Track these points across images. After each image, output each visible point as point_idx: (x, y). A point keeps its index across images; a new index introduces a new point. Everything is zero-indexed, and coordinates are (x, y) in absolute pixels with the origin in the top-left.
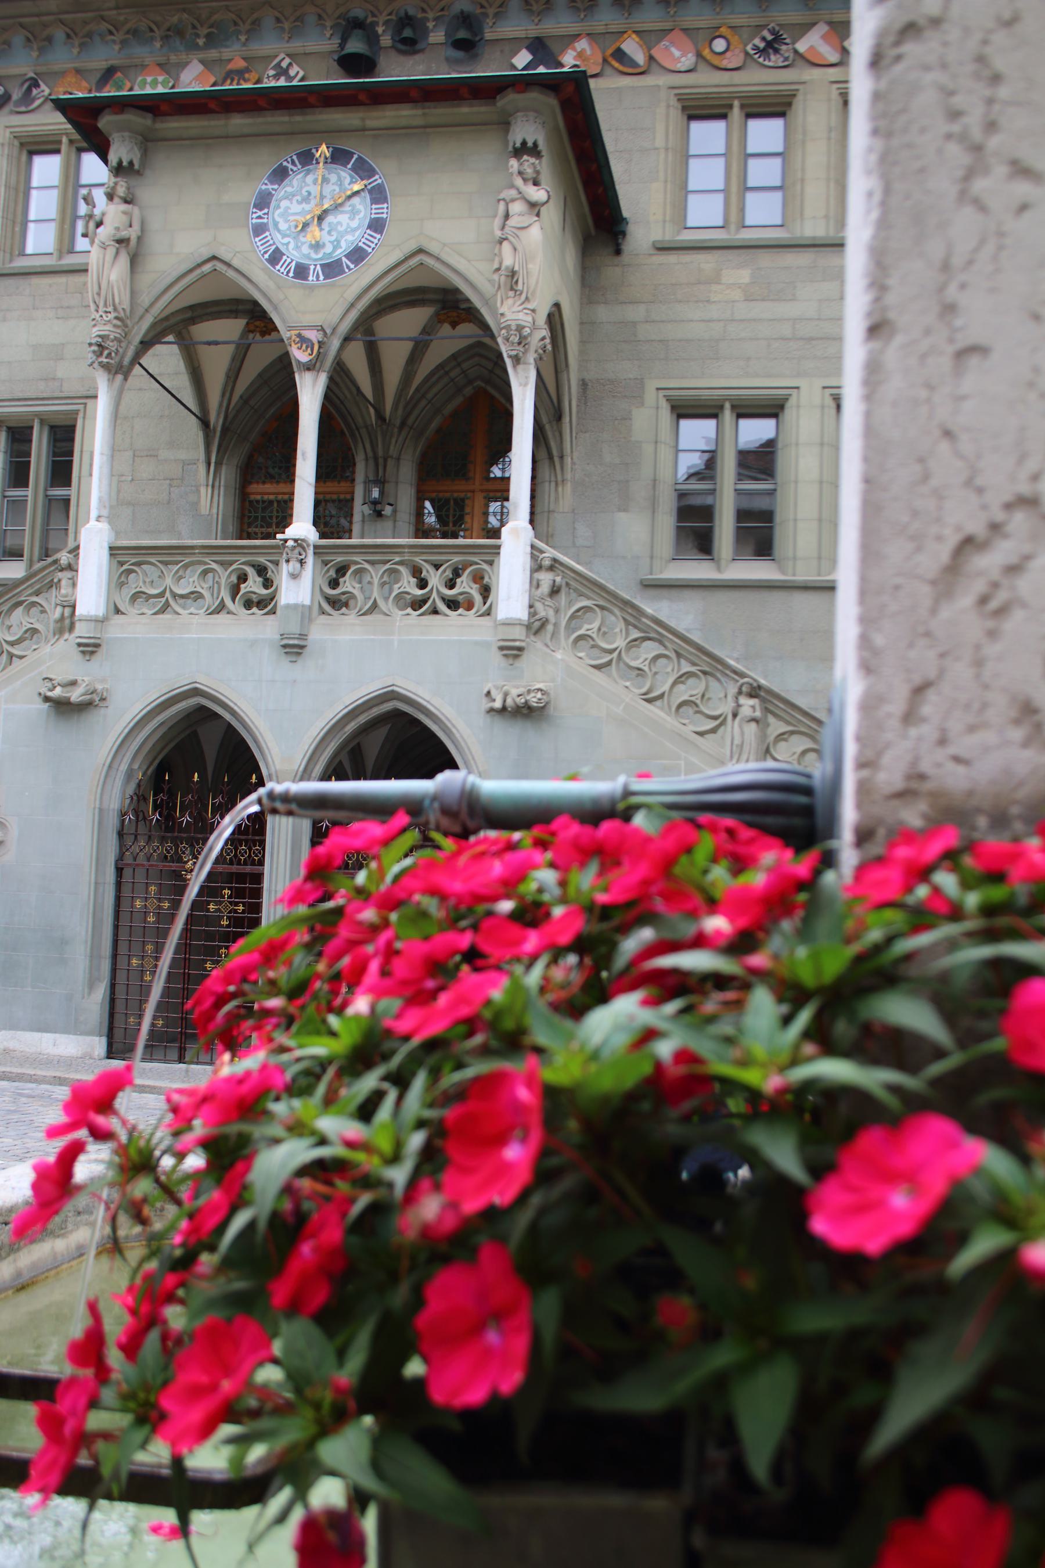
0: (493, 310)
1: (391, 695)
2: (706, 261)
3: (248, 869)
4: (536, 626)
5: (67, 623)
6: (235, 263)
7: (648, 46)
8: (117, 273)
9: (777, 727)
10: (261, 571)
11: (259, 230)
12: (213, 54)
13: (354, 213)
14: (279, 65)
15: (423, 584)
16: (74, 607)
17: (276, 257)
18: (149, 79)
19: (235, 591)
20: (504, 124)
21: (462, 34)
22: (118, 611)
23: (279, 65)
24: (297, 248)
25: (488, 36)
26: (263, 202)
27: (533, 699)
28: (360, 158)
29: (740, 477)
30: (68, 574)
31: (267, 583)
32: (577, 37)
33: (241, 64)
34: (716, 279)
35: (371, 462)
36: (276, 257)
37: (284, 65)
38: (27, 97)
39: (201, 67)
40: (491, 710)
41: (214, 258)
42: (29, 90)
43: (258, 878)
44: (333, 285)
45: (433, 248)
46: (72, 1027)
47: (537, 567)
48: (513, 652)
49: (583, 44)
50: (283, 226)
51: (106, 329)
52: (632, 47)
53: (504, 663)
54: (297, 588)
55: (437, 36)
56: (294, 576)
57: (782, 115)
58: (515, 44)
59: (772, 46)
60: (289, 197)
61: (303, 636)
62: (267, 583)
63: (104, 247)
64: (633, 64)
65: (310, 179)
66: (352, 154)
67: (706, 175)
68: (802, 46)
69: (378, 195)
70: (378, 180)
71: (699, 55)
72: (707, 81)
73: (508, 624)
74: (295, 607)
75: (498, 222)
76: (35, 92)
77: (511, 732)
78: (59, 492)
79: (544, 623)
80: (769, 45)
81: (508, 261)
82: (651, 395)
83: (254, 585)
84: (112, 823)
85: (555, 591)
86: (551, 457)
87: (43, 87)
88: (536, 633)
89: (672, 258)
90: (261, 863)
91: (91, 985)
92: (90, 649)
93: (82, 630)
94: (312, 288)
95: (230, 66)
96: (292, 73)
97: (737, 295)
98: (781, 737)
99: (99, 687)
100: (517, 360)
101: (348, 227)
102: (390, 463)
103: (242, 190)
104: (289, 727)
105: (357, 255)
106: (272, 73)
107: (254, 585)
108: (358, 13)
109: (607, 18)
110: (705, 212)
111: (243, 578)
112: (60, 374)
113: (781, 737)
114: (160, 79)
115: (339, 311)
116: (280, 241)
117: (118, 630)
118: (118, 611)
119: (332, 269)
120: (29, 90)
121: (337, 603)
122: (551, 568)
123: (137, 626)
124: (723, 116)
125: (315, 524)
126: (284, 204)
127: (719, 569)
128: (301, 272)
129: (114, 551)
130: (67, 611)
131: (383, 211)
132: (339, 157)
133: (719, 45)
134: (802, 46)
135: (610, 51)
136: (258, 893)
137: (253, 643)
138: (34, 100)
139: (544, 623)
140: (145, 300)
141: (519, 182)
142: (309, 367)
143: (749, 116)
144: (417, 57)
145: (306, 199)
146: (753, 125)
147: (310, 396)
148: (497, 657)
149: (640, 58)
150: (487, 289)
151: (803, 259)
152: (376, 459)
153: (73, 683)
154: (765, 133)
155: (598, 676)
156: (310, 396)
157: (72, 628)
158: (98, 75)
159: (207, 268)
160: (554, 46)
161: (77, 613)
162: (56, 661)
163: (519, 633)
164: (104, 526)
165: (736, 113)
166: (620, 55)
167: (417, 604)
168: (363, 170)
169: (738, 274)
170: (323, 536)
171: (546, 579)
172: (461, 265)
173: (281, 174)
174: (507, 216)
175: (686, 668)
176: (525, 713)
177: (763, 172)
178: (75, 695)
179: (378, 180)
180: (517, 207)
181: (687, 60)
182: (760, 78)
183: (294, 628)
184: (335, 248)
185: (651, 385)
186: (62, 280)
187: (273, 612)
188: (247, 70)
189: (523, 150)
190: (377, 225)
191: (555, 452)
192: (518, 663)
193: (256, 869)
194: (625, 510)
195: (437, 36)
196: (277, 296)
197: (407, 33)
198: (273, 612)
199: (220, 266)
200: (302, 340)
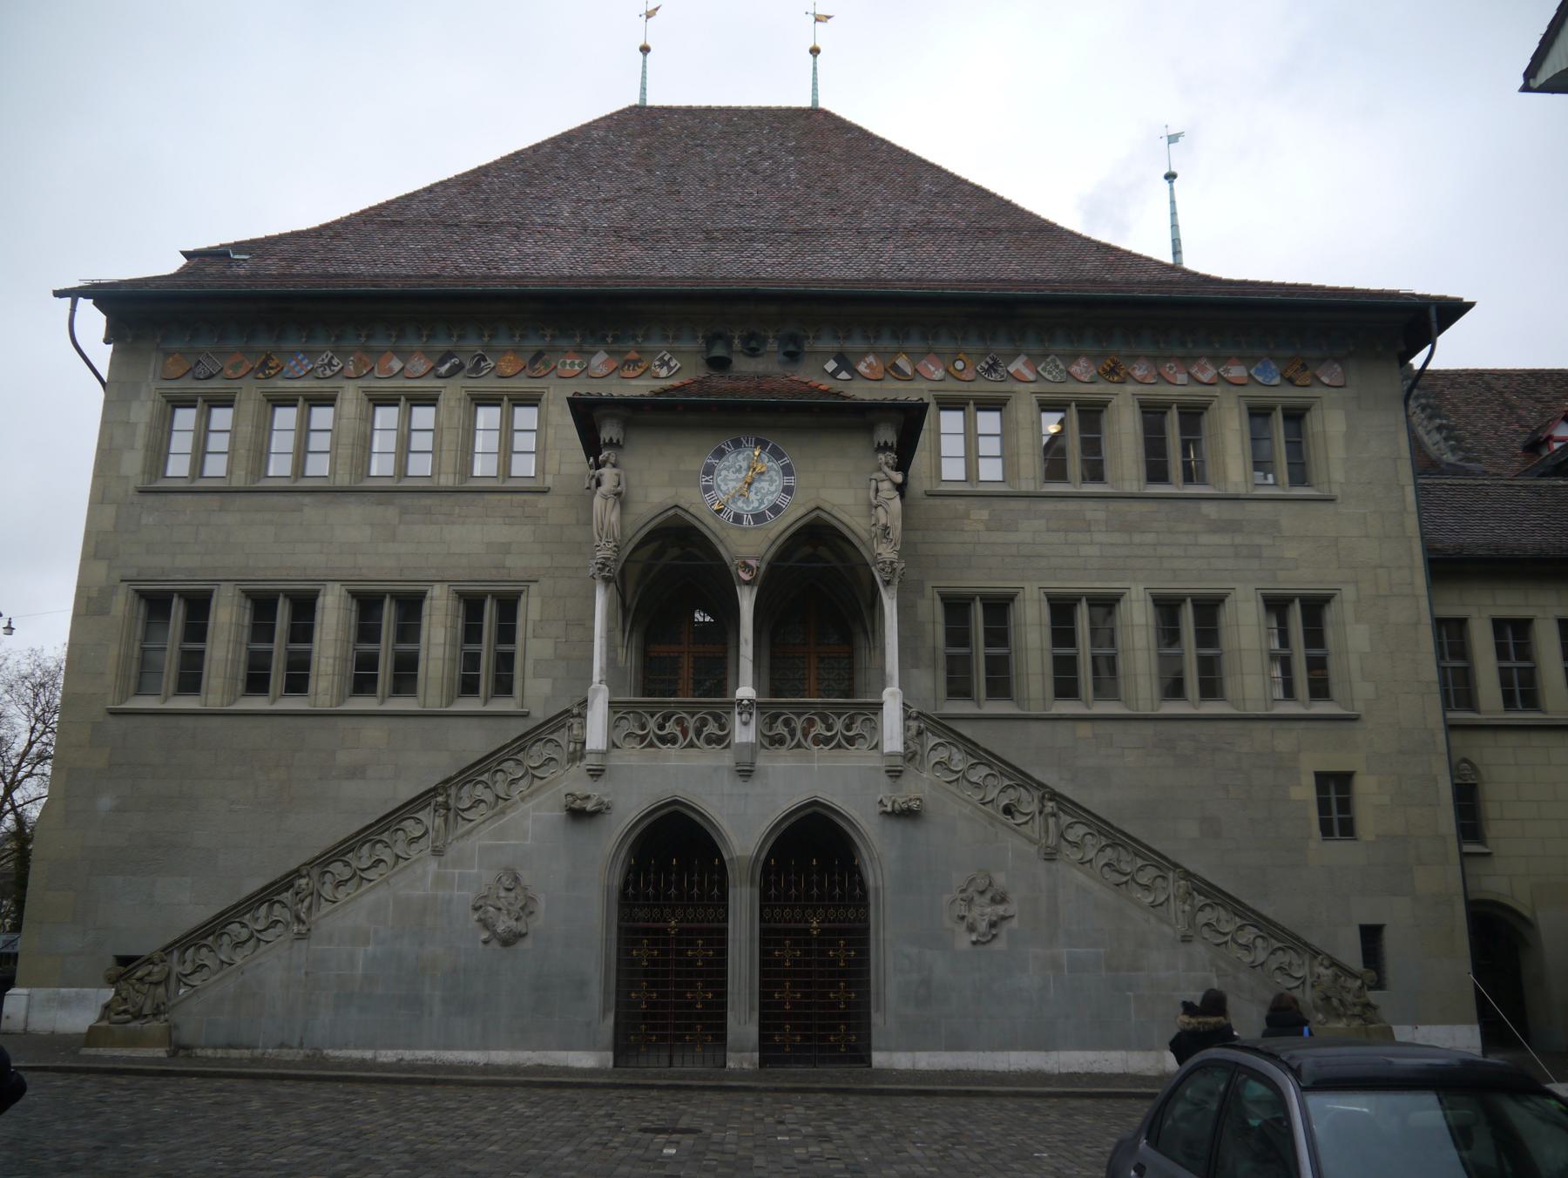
0: (871, 550)
1: (815, 803)
2: (960, 504)
3: (716, 925)
4: (910, 756)
5: (579, 753)
7: (914, 364)
8: (614, 517)
9: (1066, 819)
10: (717, 718)
11: (707, 489)
12: (615, 347)
13: (772, 481)
15: (829, 728)
16: (584, 743)
19: (698, 733)
20: (869, 429)
21: (791, 348)
22: (615, 745)
26: (709, 470)
27: (914, 805)
29: (987, 645)
30: (578, 720)
31: (722, 727)
32: (866, 354)
33: (633, 355)
34: (967, 516)
38: (477, 368)
40: (884, 813)
42: (478, 362)
43: (724, 931)
45: (827, 507)
46: (590, 1046)
47: (907, 717)
48: (895, 774)
49: (871, 359)
50: (723, 488)
51: (608, 554)
52: (903, 362)
53: (889, 780)
54: (744, 733)
55: (772, 345)
56: (746, 724)
57: (999, 410)
58: (826, 355)
59: (992, 368)
60: (727, 469)
61: (752, 764)
62: (722, 727)
63: (605, 497)
64: (905, 374)
65: (740, 457)
67: (952, 446)
68: (1012, 369)
69: (787, 471)
70: (787, 460)
71: (947, 371)
72: (953, 387)
73: (892, 755)
74: (746, 745)
75: (872, 494)
77: (897, 827)
78: (505, 648)
79: (915, 754)
80: (991, 366)
81: (883, 521)
82: (928, 591)
83: (712, 728)
84: (615, 895)
85: (920, 733)
86: (866, 632)
88: (910, 760)
89: (938, 501)
90: (726, 920)
91: (605, 1012)
92: (596, 773)
93: (591, 760)
94: (745, 529)
95: (628, 357)
97: (981, 527)
98: (1070, 826)
99: (606, 800)
100: (887, 583)
101: (769, 490)
103: (695, 464)
104: (744, 823)
105: (775, 509)
107: (712, 728)
109: (886, 343)
110: (953, 470)
111: (704, 722)
112: (508, 564)
113: (1070, 826)
115: (765, 546)
117: (616, 760)
118: (615, 745)
119: (759, 517)
120: (478, 362)
121: (778, 741)
122: (916, 718)
123: (632, 757)
124: (962, 409)
125: (757, 685)
126: (724, 473)
127: (979, 706)
128: (738, 518)
129: (611, 704)
130: (579, 746)
132: (762, 444)
133: (959, 365)
134: (1012, 369)
136: (724, 942)
137: (716, 769)
139: (915, 754)
140: (629, 533)
141: (886, 469)
142: (747, 583)
143: (979, 410)
144: (759, 359)
145: (739, 470)
146: (980, 415)
147: (747, 602)
148: (884, 778)
149: (909, 370)
150: (865, 536)
151: (1021, 505)
153: (588, 797)
154: (989, 422)
155: (952, 788)
156: (747, 602)
157: (582, 757)
158: (531, 355)
159: (671, 513)
162: (572, 781)
163: (899, 761)
164: (604, 687)
165: (972, 406)
166: (895, 367)
167: (827, 741)
168: (776, 454)
169: (981, 513)
171: (914, 724)
172: (846, 519)
173: (720, 454)
174: (877, 490)
175: (1007, 782)
176: (907, 814)
177: (989, 446)
178: (590, 806)
179: (787, 460)
180: (886, 485)
181: (939, 374)
182: (985, 387)
183: (747, 758)
184: (761, 503)
185: (929, 585)
186: (508, 497)
188: (640, 360)
189: (883, 448)
190: (788, 490)
192: (899, 781)
193: (722, 925)
194: (917, 667)
195: (772, 345)
196: (722, 534)
197: (753, 344)
198: (728, 746)
199: (680, 512)
200: (746, 567)
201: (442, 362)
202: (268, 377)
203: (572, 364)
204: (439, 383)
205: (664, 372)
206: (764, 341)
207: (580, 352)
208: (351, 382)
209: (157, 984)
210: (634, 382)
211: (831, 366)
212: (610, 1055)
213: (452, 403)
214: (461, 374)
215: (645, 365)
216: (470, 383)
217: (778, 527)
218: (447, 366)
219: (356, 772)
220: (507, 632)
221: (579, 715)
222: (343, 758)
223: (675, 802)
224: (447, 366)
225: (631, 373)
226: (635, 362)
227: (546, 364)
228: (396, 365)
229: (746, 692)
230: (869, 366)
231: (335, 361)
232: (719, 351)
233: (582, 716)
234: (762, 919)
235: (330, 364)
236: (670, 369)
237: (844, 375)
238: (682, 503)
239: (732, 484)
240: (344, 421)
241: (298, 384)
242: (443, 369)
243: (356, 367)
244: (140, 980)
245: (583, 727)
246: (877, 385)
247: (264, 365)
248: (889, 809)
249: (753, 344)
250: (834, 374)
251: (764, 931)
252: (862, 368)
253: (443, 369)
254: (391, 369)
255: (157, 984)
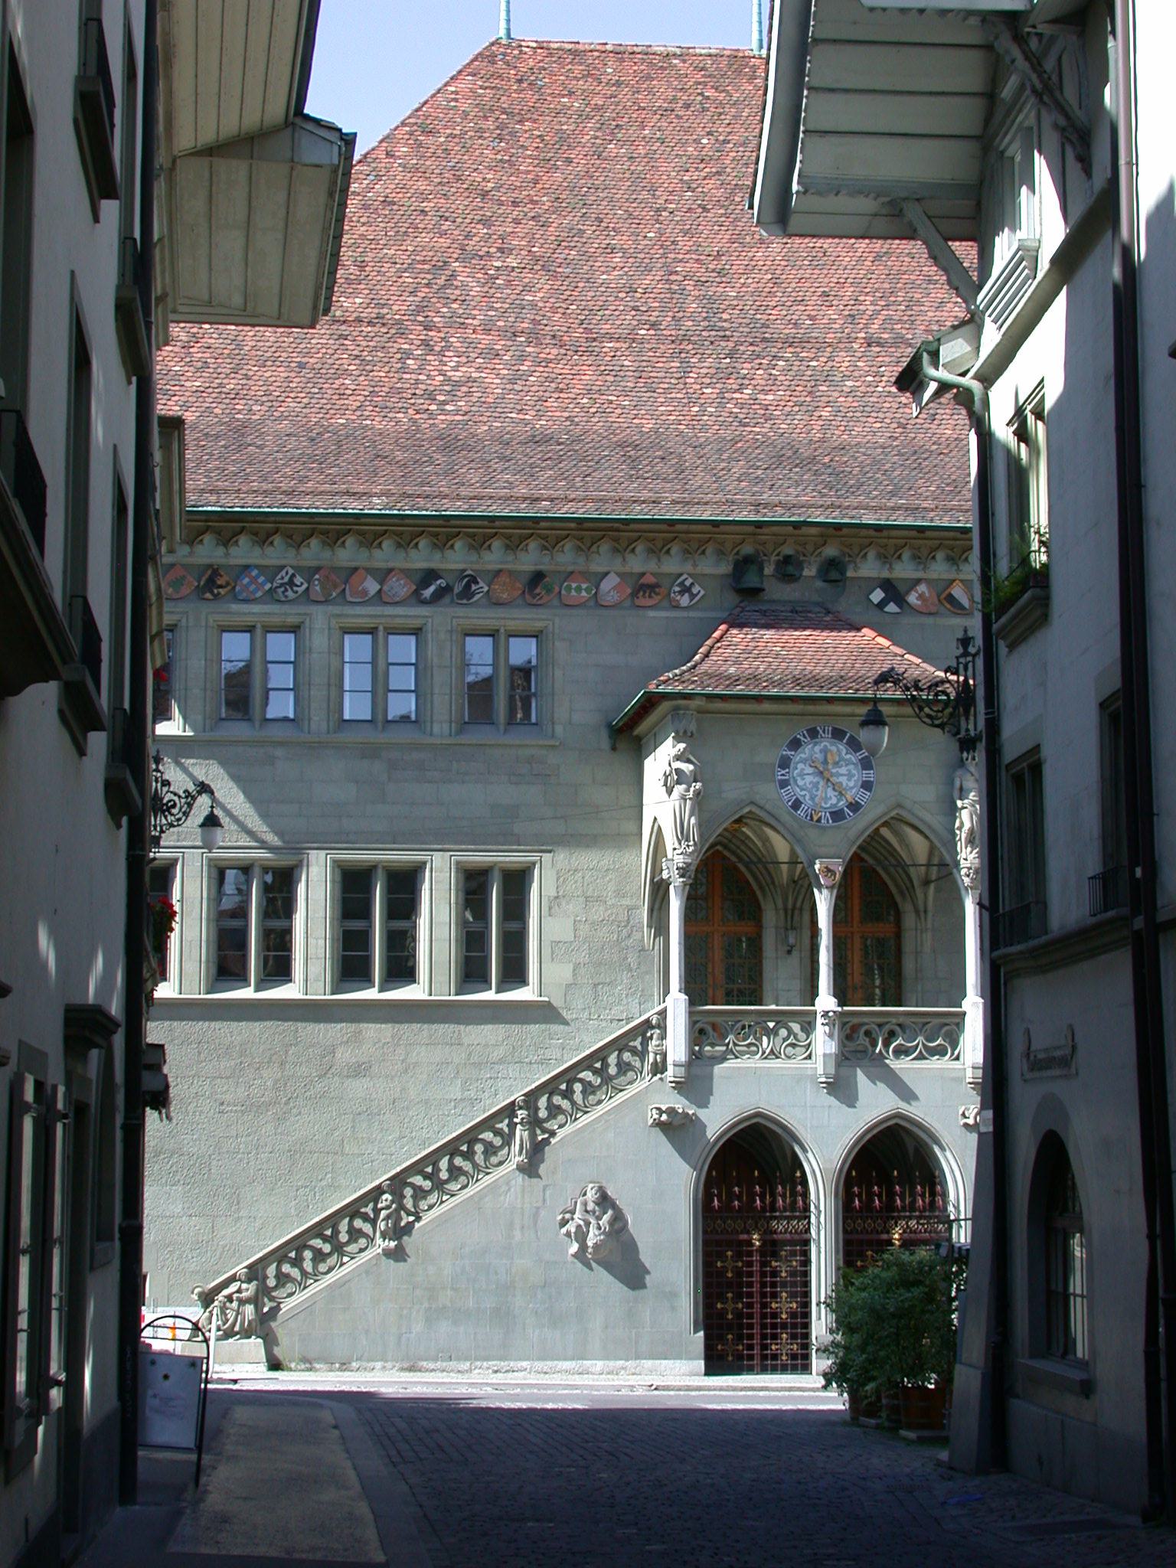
6: (767, 807)
11: (784, 784)
13: (850, 776)
14: (682, 584)
16: (664, 1055)
17: (797, 805)
18: (574, 585)
21: (834, 575)
23: (682, 584)
24: (812, 799)
25: (850, 574)
26: (785, 763)
28: (851, 737)
32: (918, 581)
33: (649, 579)
35: (782, 912)
36: (797, 805)
37: (688, 583)
38: (467, 593)
39: (618, 580)
40: (966, 1125)
41: (752, 803)
44: (838, 827)
49: (922, 588)
50: (800, 783)
54: (823, 1043)
55: (810, 571)
64: (962, 608)
65: (817, 749)
66: (845, 733)
76: (474, 587)
87: (481, 584)
94: (824, 828)
96: (695, 591)
102: (797, 912)
105: (855, 807)
106: (677, 589)
108: (747, 549)
112: (516, 831)
114: (584, 586)
116: (800, 793)
119: (838, 815)
120: (468, 586)
126: (800, 766)
131: (870, 775)
132: (838, 734)
135: (944, 596)
138: (473, 594)
152: (786, 910)
156: (823, 904)
157: (664, 1069)
160: (901, 588)
161: (670, 1060)
166: (951, 599)
170: (841, 1004)
173: (796, 744)
187: (809, 1057)
190: (867, 786)
191: (921, 908)
193: (805, 1236)
195: (810, 571)
197: (790, 569)
199: (754, 809)
201: (425, 583)
202: (216, 596)
203: (579, 589)
204: (424, 611)
205: (685, 600)
206: (800, 566)
207: (586, 575)
208: (320, 608)
209: (248, 1301)
210: (651, 613)
211: (877, 596)
212: (700, 1364)
213: (442, 636)
214: (447, 599)
215: (663, 590)
216: (460, 611)
217: (858, 826)
218: (432, 588)
219: (359, 1070)
220: (515, 909)
221: (659, 1026)
222: (345, 1056)
223: (758, 1115)
224: (432, 588)
225: (650, 602)
226: (651, 589)
227: (549, 591)
228: (372, 586)
229: (826, 1001)
230: (921, 597)
231: (298, 580)
232: (751, 580)
233: (662, 1026)
234: (845, 1231)
235: (291, 583)
236: (693, 596)
237: (892, 608)
238: (757, 798)
239: (809, 779)
240: (315, 656)
241: (256, 608)
242: (428, 593)
243: (323, 588)
244: (230, 1298)
245: (663, 1037)
246: (930, 620)
247: (211, 584)
248: (971, 1121)
249: (790, 569)
250: (881, 605)
251: (847, 1243)
252: (912, 598)
253: (428, 593)
254: (365, 592)
255: (248, 1301)
